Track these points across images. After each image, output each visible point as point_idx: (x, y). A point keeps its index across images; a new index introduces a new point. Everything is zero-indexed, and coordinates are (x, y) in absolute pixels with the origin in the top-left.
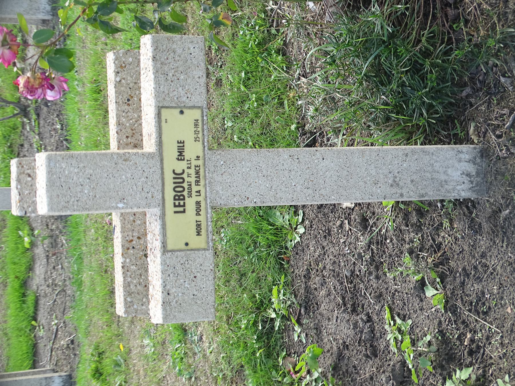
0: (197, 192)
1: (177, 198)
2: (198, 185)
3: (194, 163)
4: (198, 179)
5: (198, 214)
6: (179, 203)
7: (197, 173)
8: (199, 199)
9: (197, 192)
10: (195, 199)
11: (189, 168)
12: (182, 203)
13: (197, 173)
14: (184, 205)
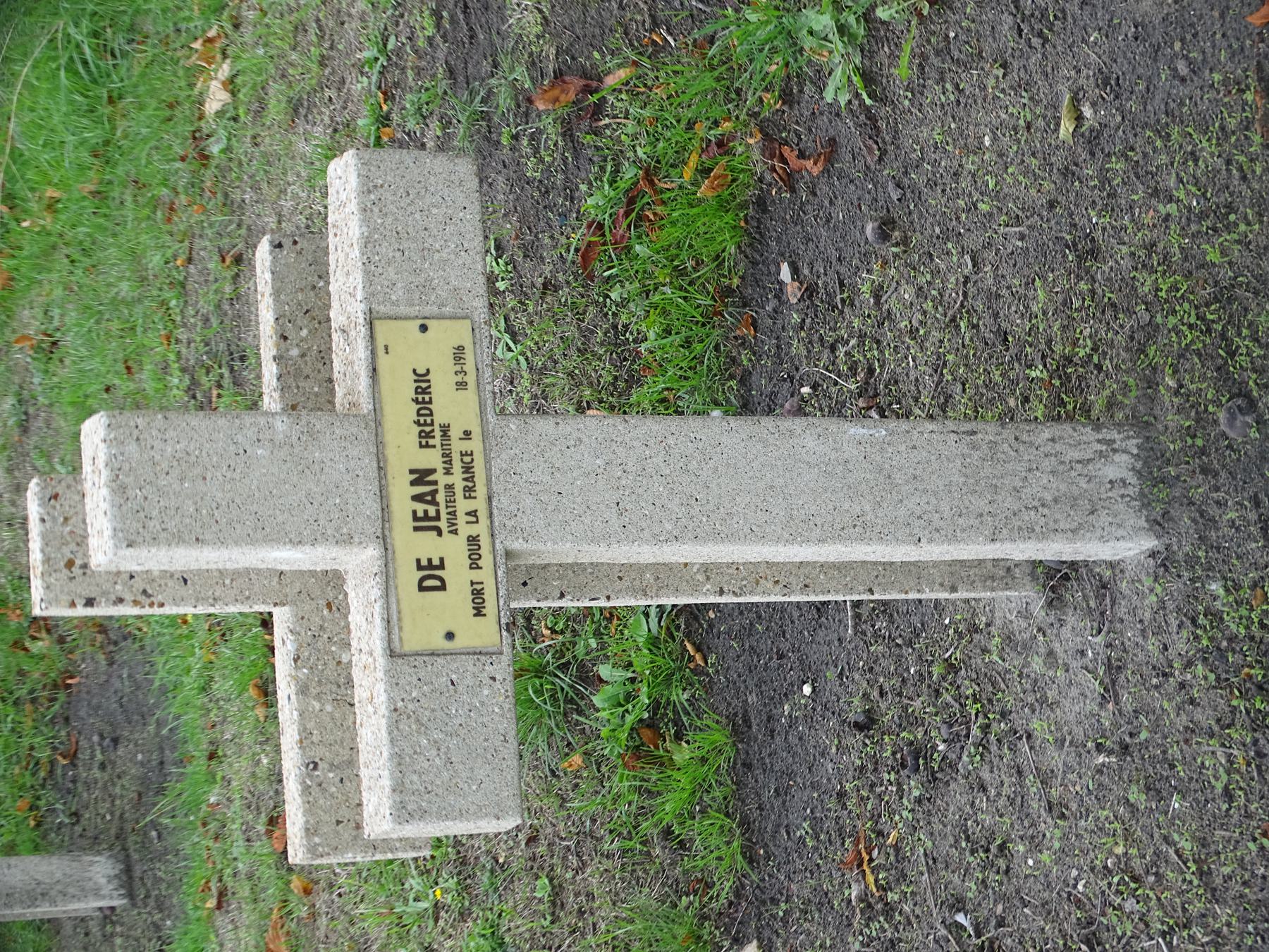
0: (468, 514)
2: (470, 497)
3: (457, 446)
4: (470, 485)
5: (475, 566)
7: (468, 469)
8: (474, 530)
9: (468, 514)
10: (465, 531)
13: (468, 469)
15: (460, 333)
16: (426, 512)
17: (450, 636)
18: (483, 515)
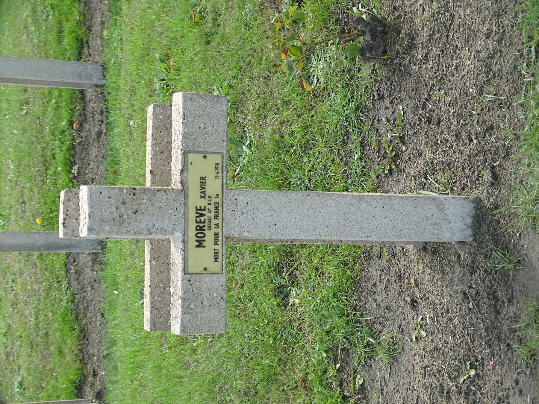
0: (215, 225)
1: (198, 228)
2: (216, 219)
3: (214, 200)
5: (216, 244)
9: (215, 225)
10: (214, 230)
11: (210, 204)
13: (216, 208)
15: (217, 159)
16: (200, 220)
18: (220, 226)
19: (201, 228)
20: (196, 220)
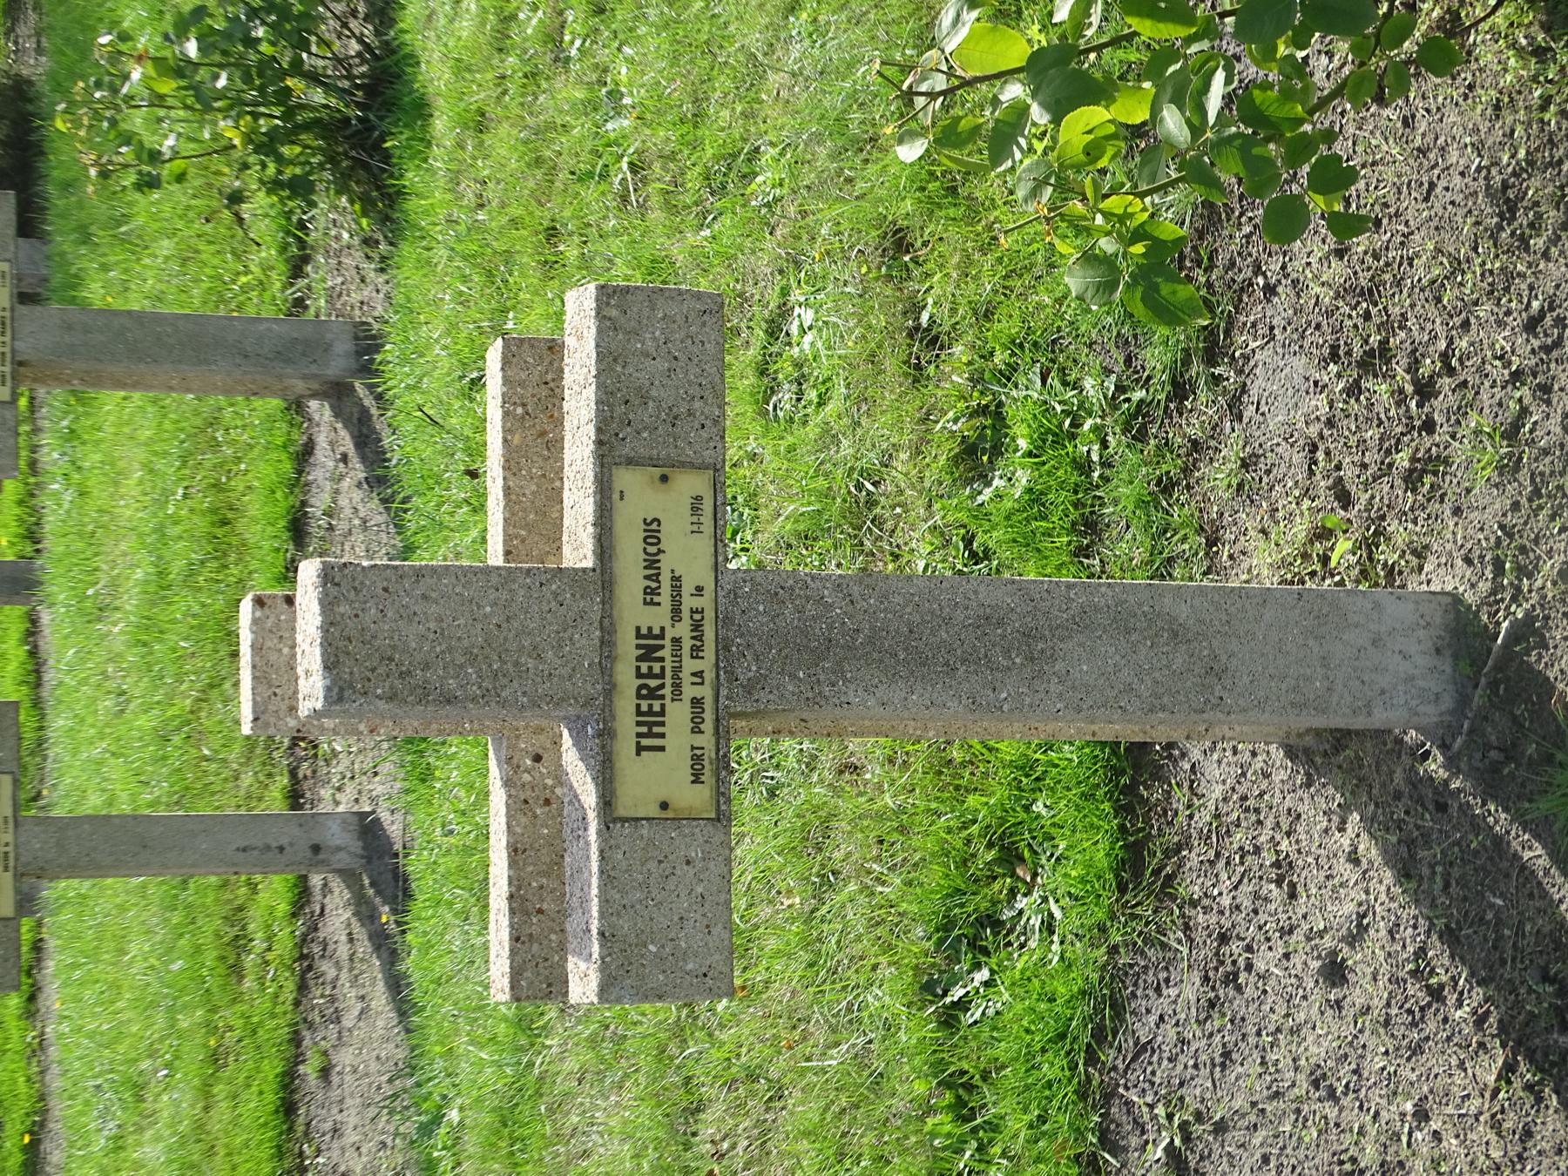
0: (694, 674)
1: (644, 692)
2: (697, 657)
3: (688, 602)
5: (697, 730)
6: (650, 706)
7: (697, 627)
8: (697, 692)
9: (694, 674)
10: (689, 691)
12: (657, 708)
13: (697, 627)
14: (662, 713)
16: (650, 668)
17: (664, 806)
19: (653, 694)
20: (638, 668)
